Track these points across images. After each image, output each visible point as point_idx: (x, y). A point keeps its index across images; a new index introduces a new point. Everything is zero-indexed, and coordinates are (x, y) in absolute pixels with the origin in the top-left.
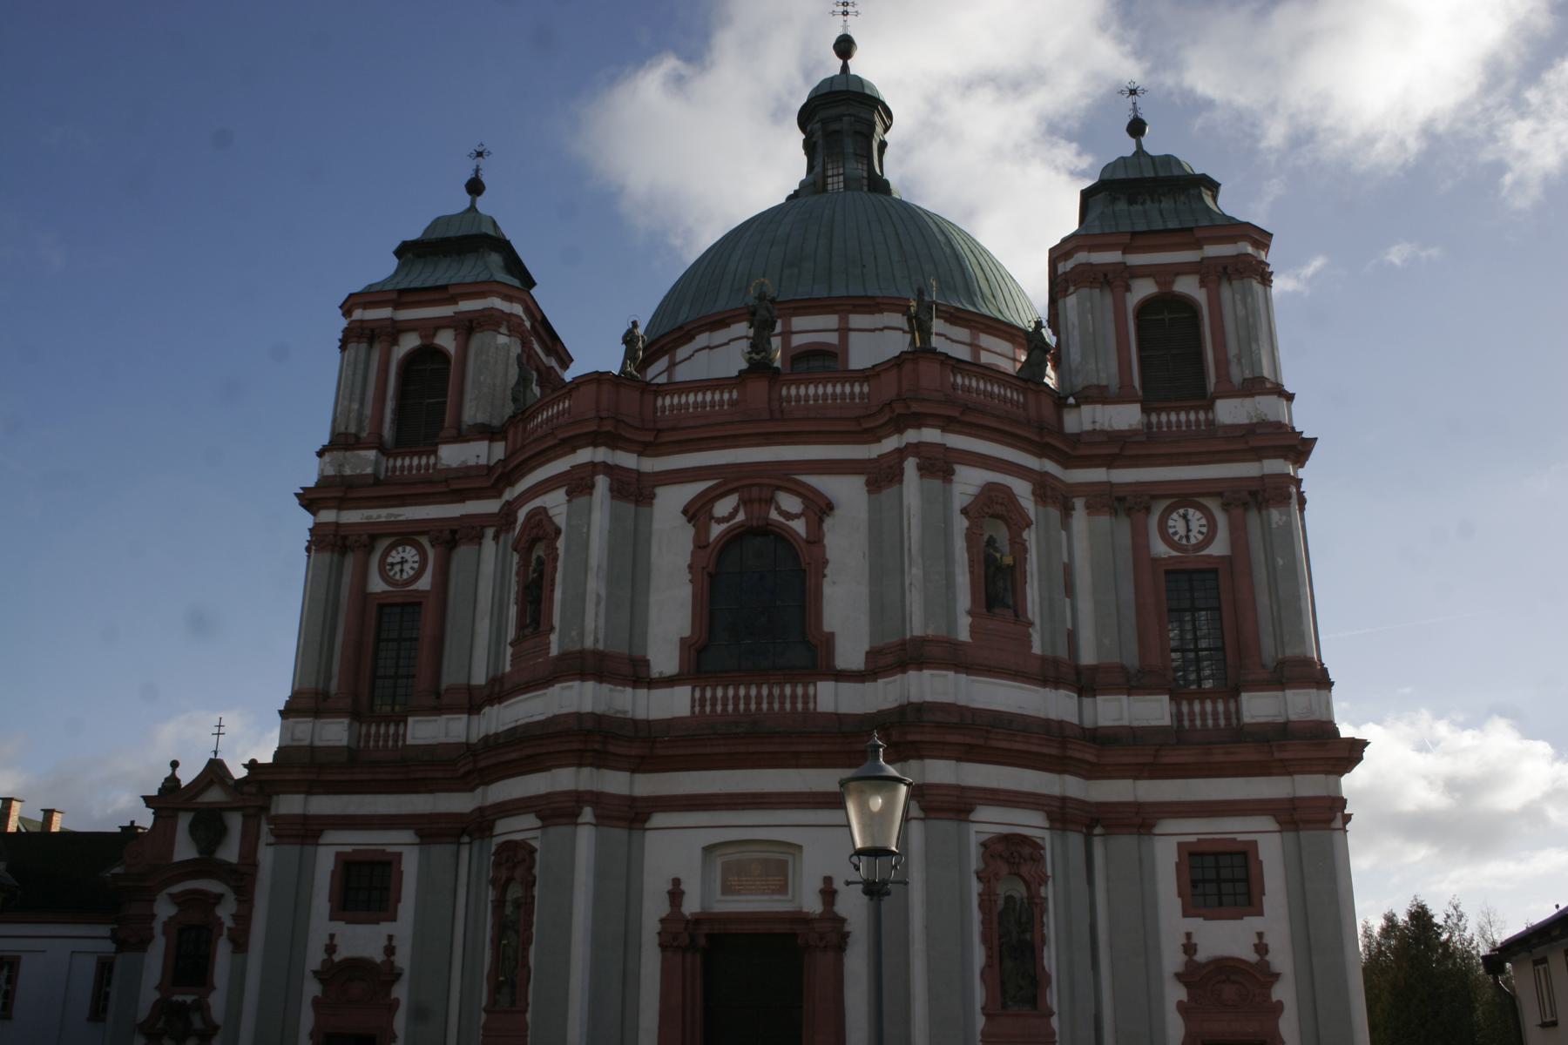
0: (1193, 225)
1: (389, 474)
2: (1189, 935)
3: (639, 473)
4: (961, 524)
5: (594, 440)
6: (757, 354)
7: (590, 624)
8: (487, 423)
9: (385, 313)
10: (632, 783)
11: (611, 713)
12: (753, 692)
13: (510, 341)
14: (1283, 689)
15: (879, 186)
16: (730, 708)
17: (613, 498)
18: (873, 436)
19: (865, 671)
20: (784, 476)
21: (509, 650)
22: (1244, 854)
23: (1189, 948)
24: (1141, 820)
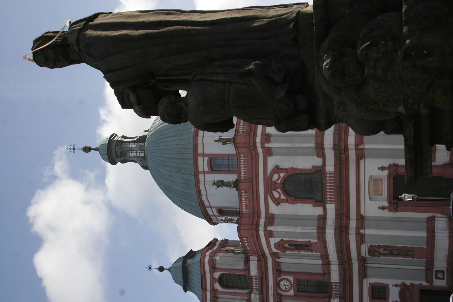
1: (258, 290)
3: (266, 218)
5: (257, 230)
6: (232, 186)
7: (310, 231)
8: (244, 261)
9: (208, 294)
10: (353, 220)
11: (334, 225)
12: (328, 187)
13: (218, 256)
15: (142, 139)
16: (332, 193)
17: (273, 225)
18: (257, 154)
19: (323, 158)
21: (314, 253)
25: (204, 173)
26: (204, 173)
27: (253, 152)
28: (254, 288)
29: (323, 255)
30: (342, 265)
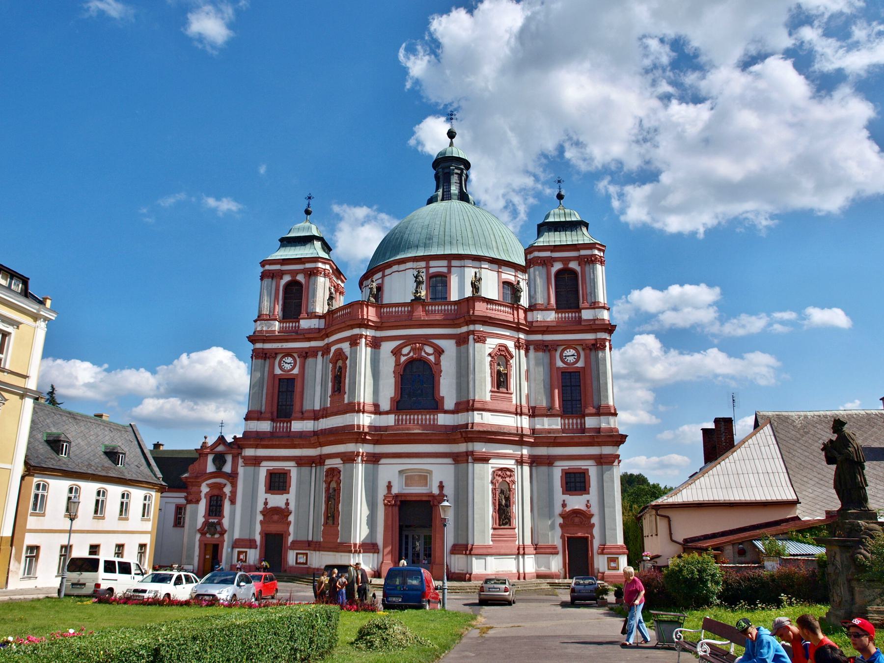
0: (577, 243)
2: (564, 501)
10: (374, 449)
12: (416, 417)
14: (600, 416)
18: (459, 326)
20: (426, 340)
22: (584, 473)
23: (564, 505)
24: (549, 461)
25: (428, 268)
26: (428, 268)
27: (462, 320)
28: (285, 325)
29: (326, 411)
30: (314, 435)
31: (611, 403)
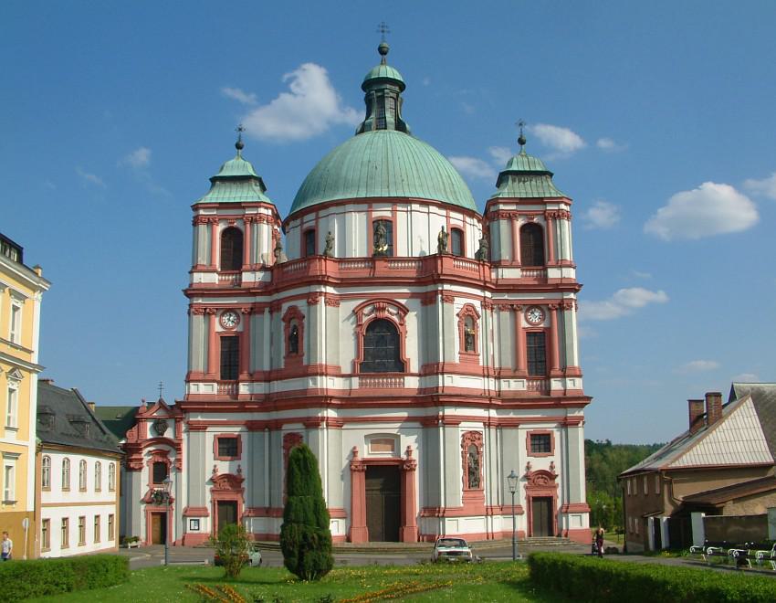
2: (528, 463)
4: (457, 319)
21: (283, 361)
31: (576, 364)
